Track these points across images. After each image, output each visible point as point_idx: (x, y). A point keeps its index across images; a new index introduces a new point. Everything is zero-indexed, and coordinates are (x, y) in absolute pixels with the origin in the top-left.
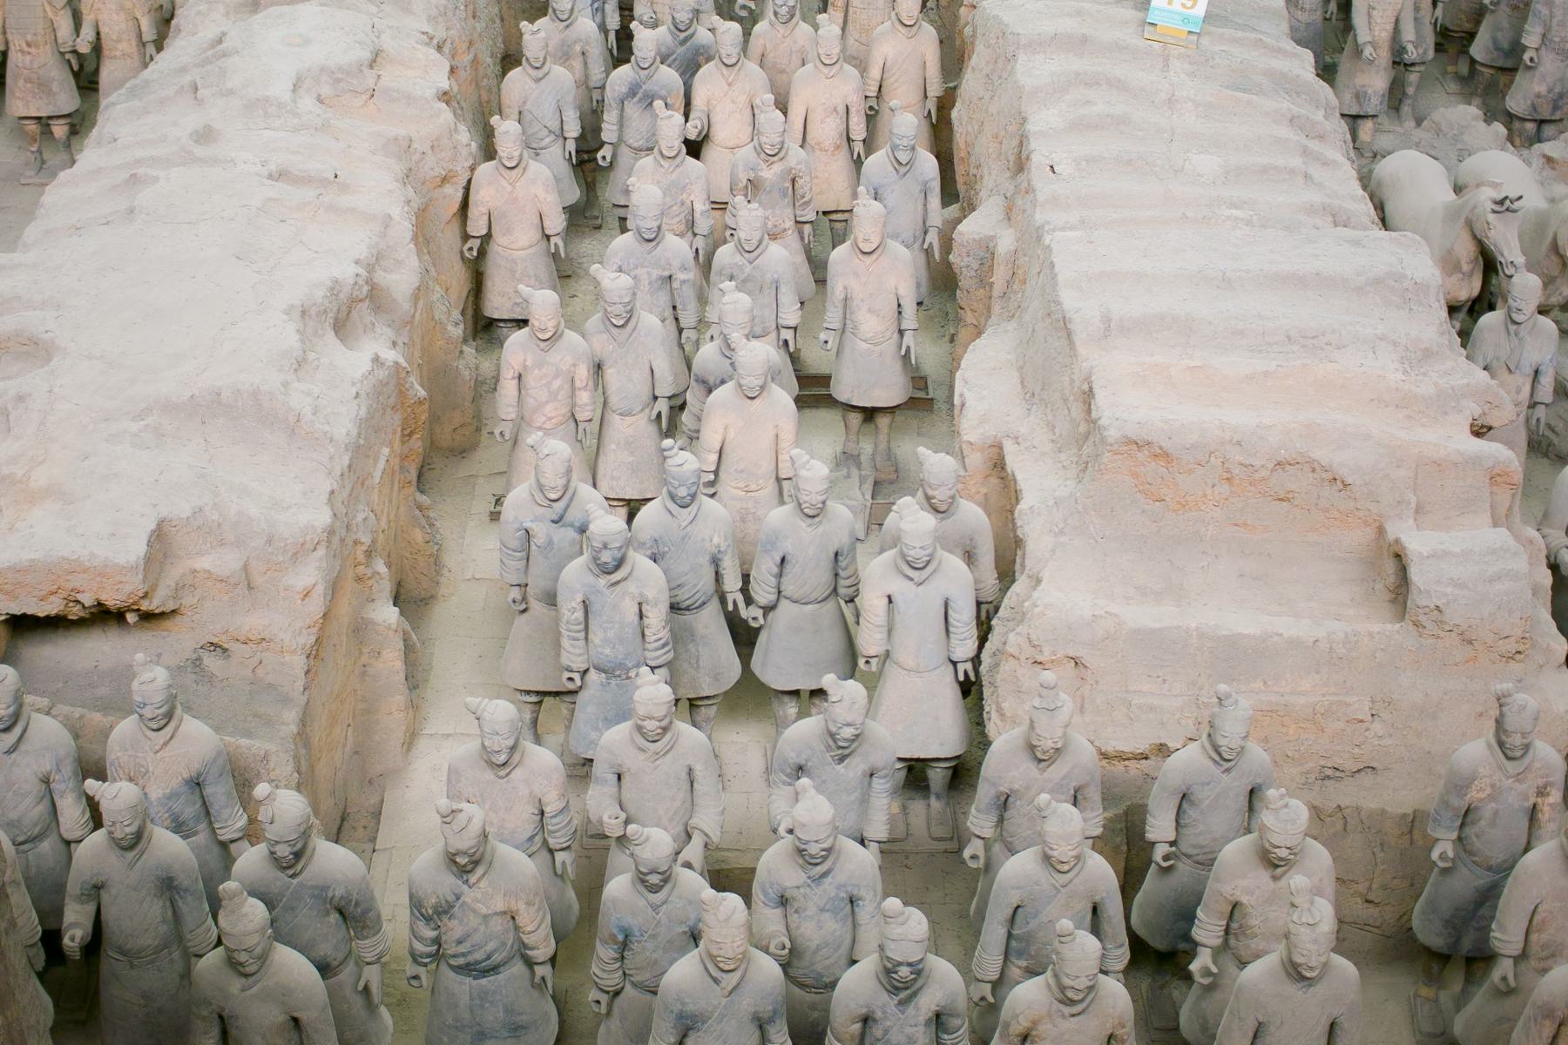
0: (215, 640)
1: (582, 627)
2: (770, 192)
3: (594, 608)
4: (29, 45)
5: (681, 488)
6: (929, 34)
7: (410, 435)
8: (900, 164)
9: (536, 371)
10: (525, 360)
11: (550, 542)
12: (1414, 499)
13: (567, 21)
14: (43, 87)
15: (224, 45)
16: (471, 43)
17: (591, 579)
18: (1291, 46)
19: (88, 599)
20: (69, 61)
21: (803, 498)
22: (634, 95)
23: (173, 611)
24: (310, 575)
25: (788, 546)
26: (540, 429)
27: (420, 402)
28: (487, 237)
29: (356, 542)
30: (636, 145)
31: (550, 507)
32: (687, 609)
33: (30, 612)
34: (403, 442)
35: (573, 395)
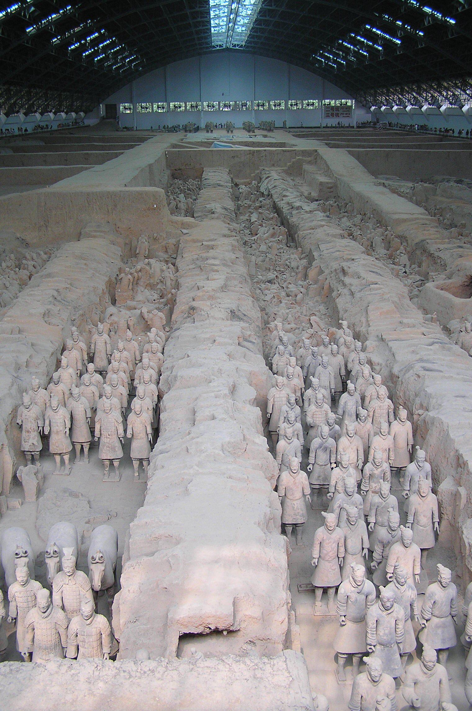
0: (251, 640)
1: (375, 630)
2: (377, 478)
4: (109, 435)
5: (403, 579)
6: (409, 424)
8: (420, 466)
9: (327, 541)
10: (323, 537)
11: (356, 600)
14: (113, 449)
15: (192, 435)
17: (380, 612)
20: (121, 441)
21: (443, 580)
22: (321, 447)
25: (437, 598)
26: (327, 561)
30: (321, 464)
31: (357, 587)
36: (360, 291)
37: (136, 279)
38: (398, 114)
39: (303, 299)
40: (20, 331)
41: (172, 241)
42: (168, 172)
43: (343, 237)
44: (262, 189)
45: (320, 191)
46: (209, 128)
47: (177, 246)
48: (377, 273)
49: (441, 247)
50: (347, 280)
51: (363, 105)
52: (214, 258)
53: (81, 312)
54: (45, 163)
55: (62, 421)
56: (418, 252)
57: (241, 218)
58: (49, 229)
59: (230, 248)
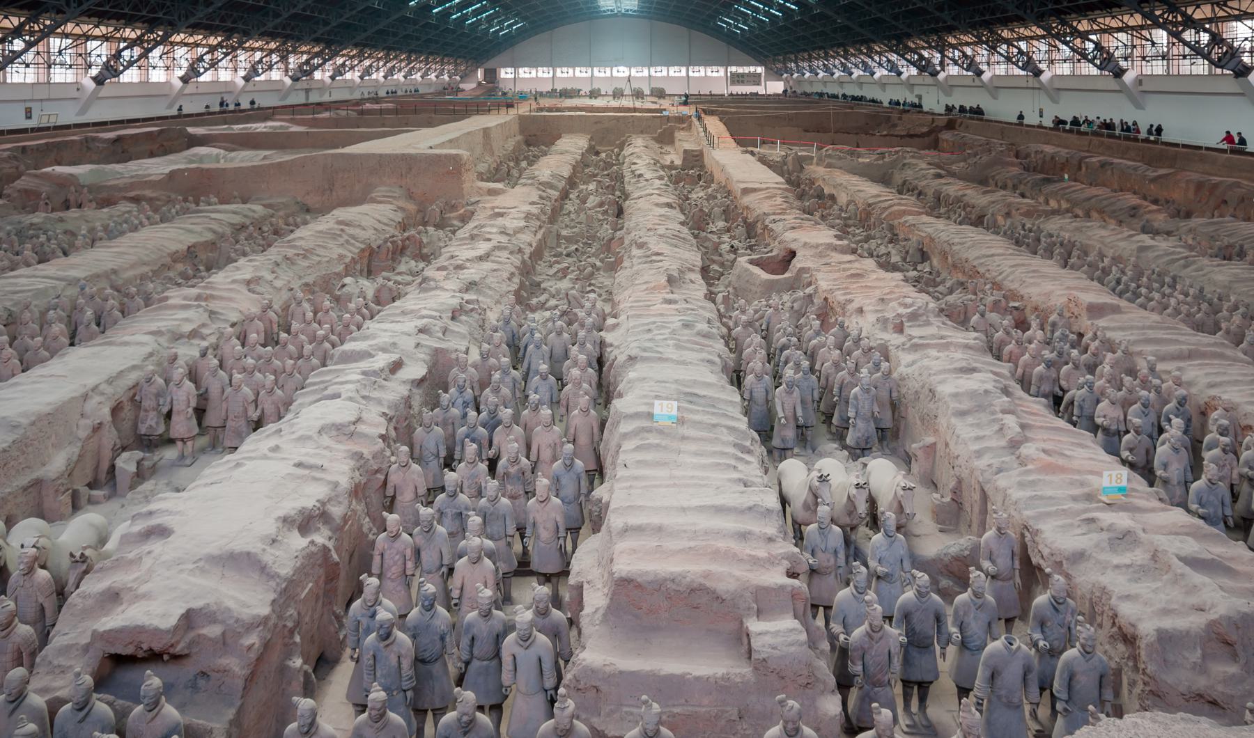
3: (377, 659)
7: (332, 580)
12: (756, 606)
13: (446, 409)
16: (406, 419)
18: (742, 417)
19: (145, 647)
23: (187, 656)
24: (253, 639)
25: (475, 631)
27: (337, 564)
28: (393, 498)
29: (285, 626)
32: (429, 662)
33: (119, 652)
34: (326, 584)
35: (405, 564)
36: (640, 263)
37: (400, 247)
38: (811, 82)
39: (592, 274)
40: (208, 298)
41: (470, 208)
42: (519, 138)
43: (669, 205)
44: (620, 158)
45: (684, 159)
46: (594, 94)
47: (473, 213)
48: (672, 245)
49: (777, 217)
50: (636, 252)
51: (776, 73)
52: (492, 226)
53: (303, 281)
54: (383, 125)
55: (184, 398)
56: (759, 225)
57: (581, 187)
58: (334, 193)
59: (523, 215)
